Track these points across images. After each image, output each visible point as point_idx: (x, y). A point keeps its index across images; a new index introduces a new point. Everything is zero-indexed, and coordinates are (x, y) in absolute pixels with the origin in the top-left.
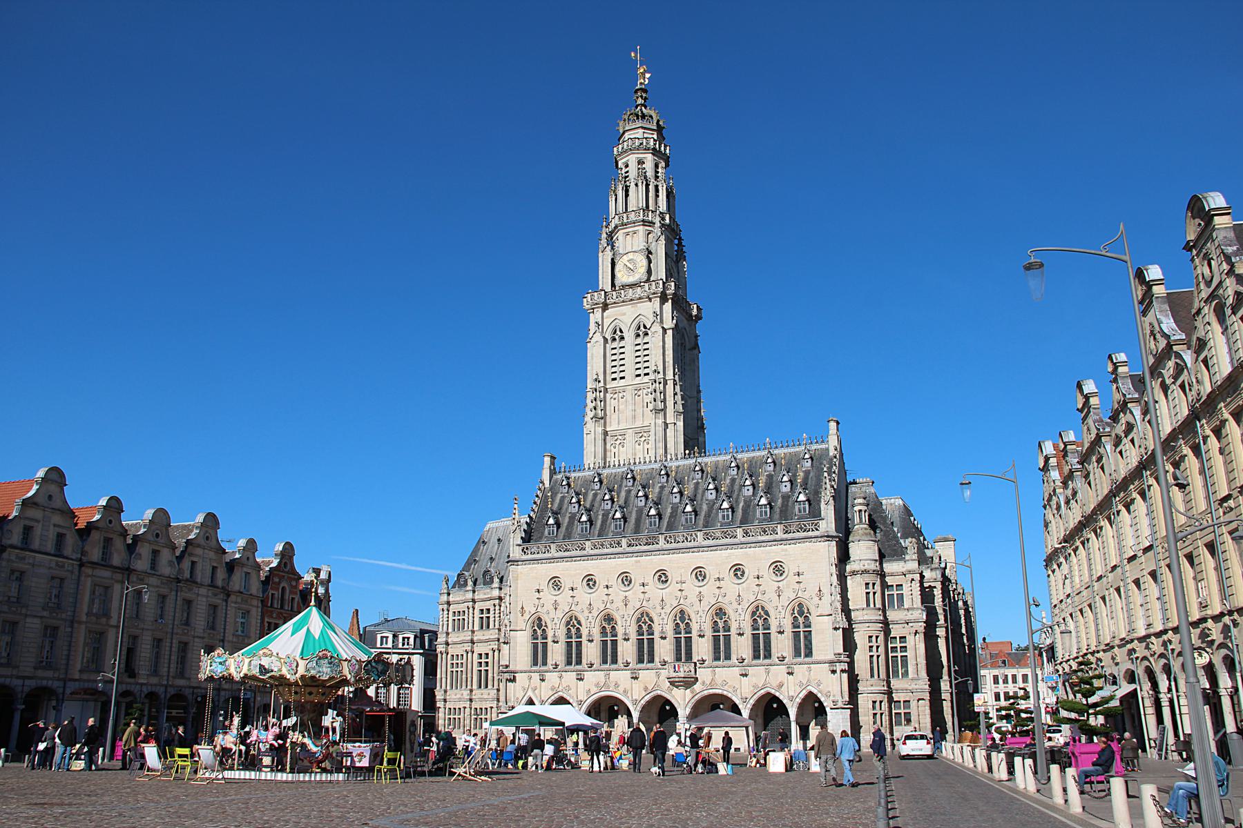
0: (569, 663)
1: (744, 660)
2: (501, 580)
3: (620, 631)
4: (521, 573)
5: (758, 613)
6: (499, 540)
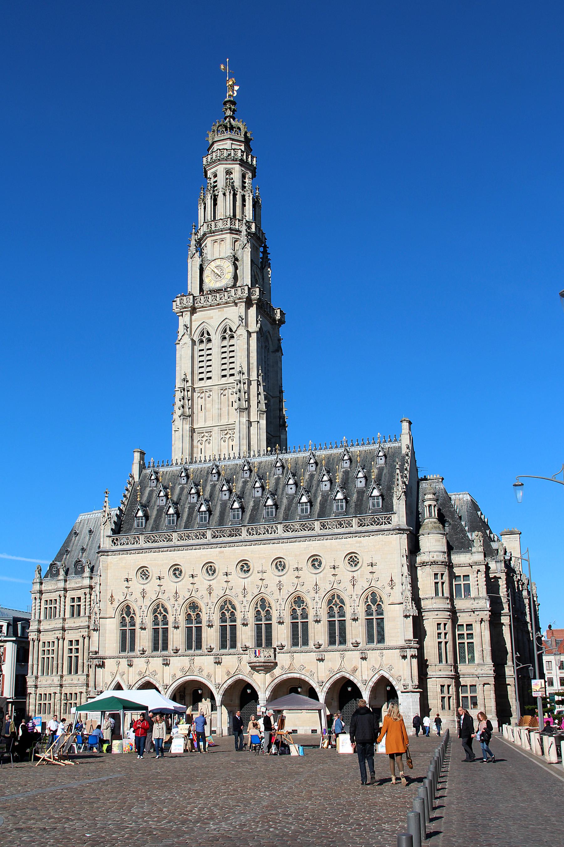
0: (156, 648)
1: (320, 645)
2: (92, 569)
3: (204, 618)
4: (111, 563)
5: (334, 601)
6: (90, 531)
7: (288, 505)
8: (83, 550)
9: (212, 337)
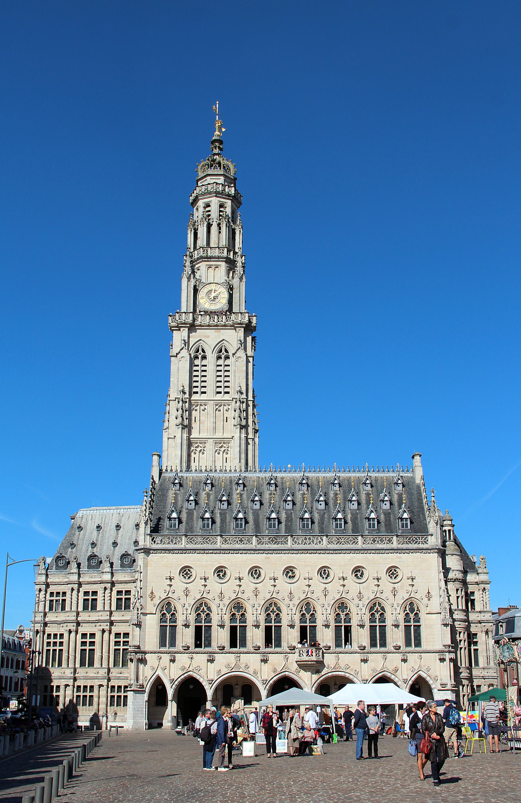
0: (198, 645)
6: (99, 527)
7: (320, 519)
8: (94, 545)
9: (208, 353)
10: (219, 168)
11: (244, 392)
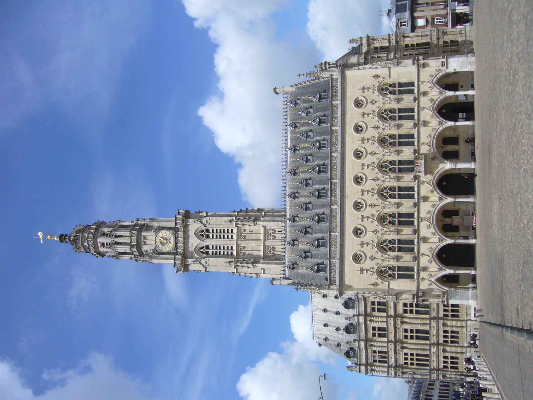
0: (412, 250)
5: (386, 116)
6: (325, 325)
8: (338, 329)
9: (204, 244)
10: (78, 237)
11: (231, 218)
